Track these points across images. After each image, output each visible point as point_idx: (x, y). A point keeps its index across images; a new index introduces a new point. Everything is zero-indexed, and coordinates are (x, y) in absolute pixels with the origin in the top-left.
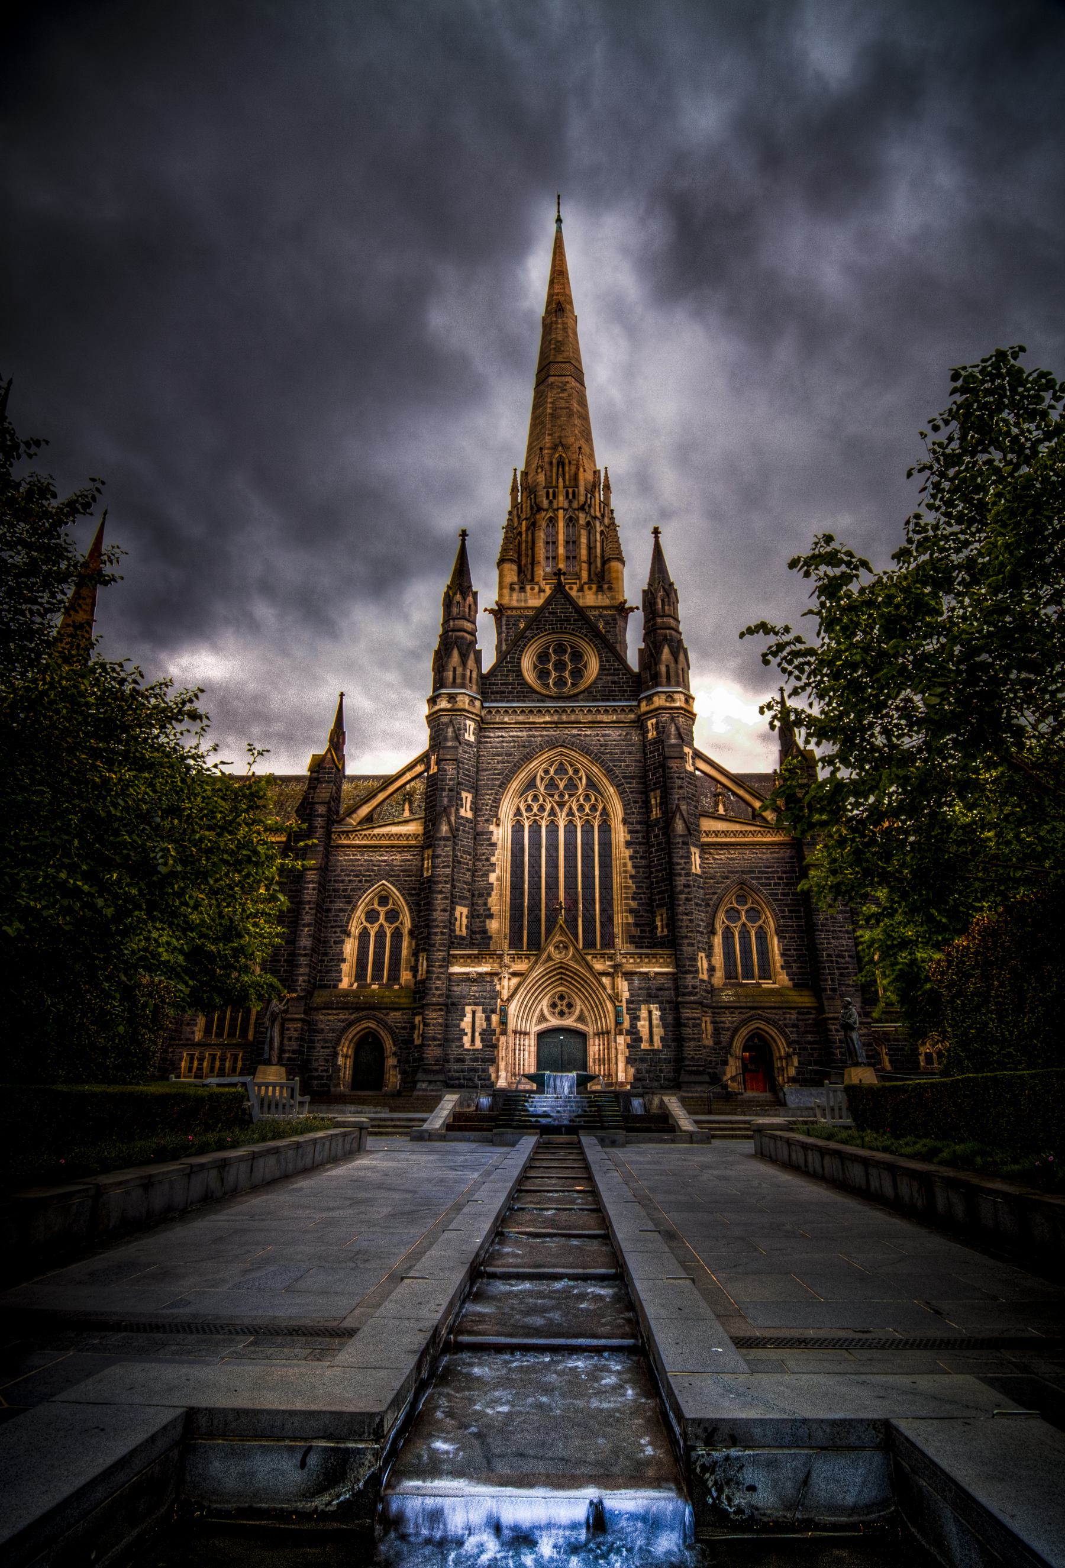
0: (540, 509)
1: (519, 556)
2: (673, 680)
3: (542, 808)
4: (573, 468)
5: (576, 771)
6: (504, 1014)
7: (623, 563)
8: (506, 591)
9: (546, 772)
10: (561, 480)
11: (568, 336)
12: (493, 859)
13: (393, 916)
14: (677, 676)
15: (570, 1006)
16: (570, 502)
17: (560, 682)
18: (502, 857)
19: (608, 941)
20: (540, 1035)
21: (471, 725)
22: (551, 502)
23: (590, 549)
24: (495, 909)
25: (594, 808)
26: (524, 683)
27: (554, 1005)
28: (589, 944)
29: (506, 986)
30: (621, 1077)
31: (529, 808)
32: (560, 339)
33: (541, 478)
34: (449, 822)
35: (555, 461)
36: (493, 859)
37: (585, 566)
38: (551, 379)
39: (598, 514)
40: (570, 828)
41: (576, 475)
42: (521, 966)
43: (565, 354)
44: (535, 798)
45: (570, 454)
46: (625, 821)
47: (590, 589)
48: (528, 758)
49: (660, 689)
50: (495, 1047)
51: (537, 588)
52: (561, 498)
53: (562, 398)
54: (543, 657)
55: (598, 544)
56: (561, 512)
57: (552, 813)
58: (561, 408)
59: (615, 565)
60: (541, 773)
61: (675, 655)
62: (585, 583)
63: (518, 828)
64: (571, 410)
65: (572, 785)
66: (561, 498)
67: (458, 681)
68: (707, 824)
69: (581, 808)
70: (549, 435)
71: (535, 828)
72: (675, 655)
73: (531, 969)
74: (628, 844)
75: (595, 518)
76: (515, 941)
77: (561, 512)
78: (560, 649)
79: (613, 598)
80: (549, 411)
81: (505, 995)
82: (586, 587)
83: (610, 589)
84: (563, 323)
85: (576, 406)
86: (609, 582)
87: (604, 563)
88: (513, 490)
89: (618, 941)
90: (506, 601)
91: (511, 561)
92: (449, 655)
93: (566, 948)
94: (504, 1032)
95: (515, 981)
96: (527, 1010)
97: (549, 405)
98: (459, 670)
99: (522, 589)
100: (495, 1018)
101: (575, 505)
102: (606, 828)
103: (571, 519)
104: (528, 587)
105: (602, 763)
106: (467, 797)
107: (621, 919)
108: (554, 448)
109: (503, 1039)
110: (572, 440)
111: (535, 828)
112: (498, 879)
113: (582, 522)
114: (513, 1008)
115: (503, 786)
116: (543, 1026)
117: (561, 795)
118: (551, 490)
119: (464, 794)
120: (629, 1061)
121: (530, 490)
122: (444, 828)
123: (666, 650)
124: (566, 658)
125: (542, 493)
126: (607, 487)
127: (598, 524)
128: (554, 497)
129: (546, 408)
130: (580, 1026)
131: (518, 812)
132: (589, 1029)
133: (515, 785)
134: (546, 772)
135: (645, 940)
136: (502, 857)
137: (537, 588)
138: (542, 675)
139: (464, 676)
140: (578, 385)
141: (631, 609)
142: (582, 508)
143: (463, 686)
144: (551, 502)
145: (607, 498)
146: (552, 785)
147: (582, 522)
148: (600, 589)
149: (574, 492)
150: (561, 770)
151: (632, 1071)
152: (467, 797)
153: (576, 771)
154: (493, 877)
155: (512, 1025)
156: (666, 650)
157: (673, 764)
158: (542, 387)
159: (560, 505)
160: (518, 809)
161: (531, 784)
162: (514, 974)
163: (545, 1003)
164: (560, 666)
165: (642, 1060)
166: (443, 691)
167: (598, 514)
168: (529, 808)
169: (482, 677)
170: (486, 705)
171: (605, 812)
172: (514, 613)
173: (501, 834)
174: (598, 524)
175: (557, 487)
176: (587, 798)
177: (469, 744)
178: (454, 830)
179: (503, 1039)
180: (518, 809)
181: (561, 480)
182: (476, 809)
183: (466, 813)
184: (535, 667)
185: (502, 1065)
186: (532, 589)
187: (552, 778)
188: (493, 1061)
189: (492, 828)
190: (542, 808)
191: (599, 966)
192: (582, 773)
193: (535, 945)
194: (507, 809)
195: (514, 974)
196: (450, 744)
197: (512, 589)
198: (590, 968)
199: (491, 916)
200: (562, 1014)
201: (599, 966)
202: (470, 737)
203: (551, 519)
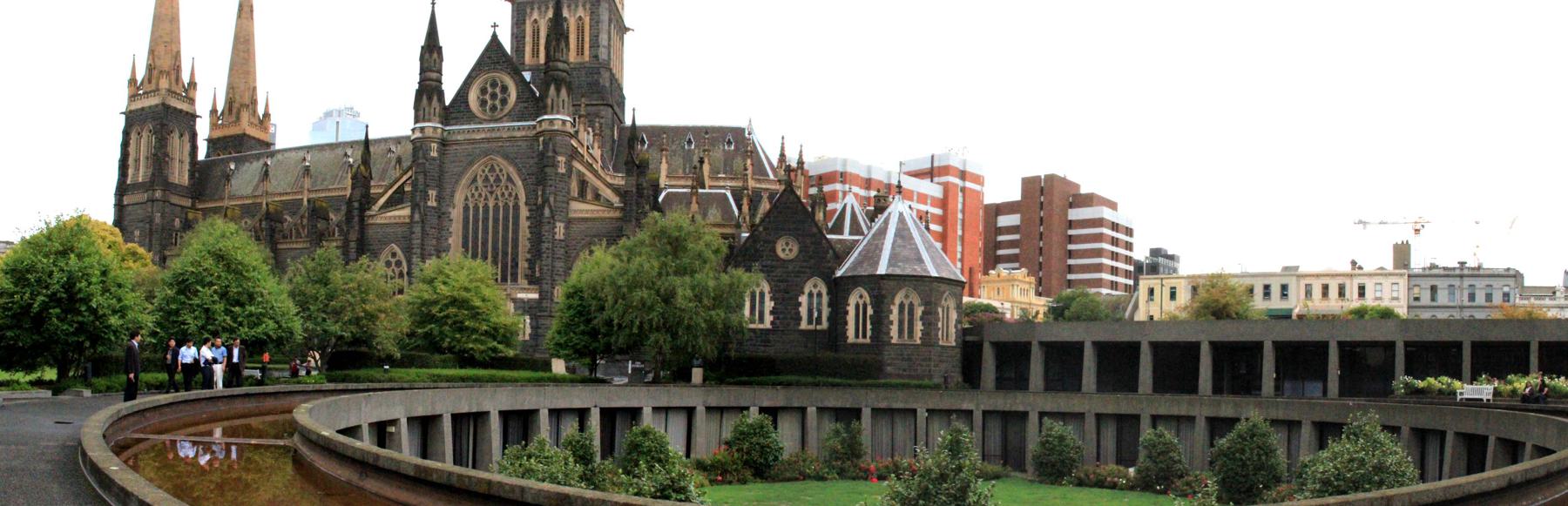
13: (399, 264)
17: (494, 108)
19: (515, 280)
21: (434, 146)
26: (469, 111)
48: (471, 164)
63: (466, 208)
65: (498, 180)
68: (575, 205)
71: (476, 208)
78: (494, 85)
102: (516, 207)
105: (516, 165)
106: (432, 193)
107: (523, 265)
111: (476, 208)
115: (457, 182)
124: (498, 90)
133: (464, 181)
135: (533, 280)
138: (483, 103)
146: (486, 179)
150: (492, 169)
152: (432, 193)
154: (450, 241)
157: (548, 170)
161: (474, 180)
164: (494, 96)
169: (445, 108)
171: (516, 197)
173: (456, 213)
177: (434, 159)
183: (432, 203)
194: (459, 198)
202: (434, 154)
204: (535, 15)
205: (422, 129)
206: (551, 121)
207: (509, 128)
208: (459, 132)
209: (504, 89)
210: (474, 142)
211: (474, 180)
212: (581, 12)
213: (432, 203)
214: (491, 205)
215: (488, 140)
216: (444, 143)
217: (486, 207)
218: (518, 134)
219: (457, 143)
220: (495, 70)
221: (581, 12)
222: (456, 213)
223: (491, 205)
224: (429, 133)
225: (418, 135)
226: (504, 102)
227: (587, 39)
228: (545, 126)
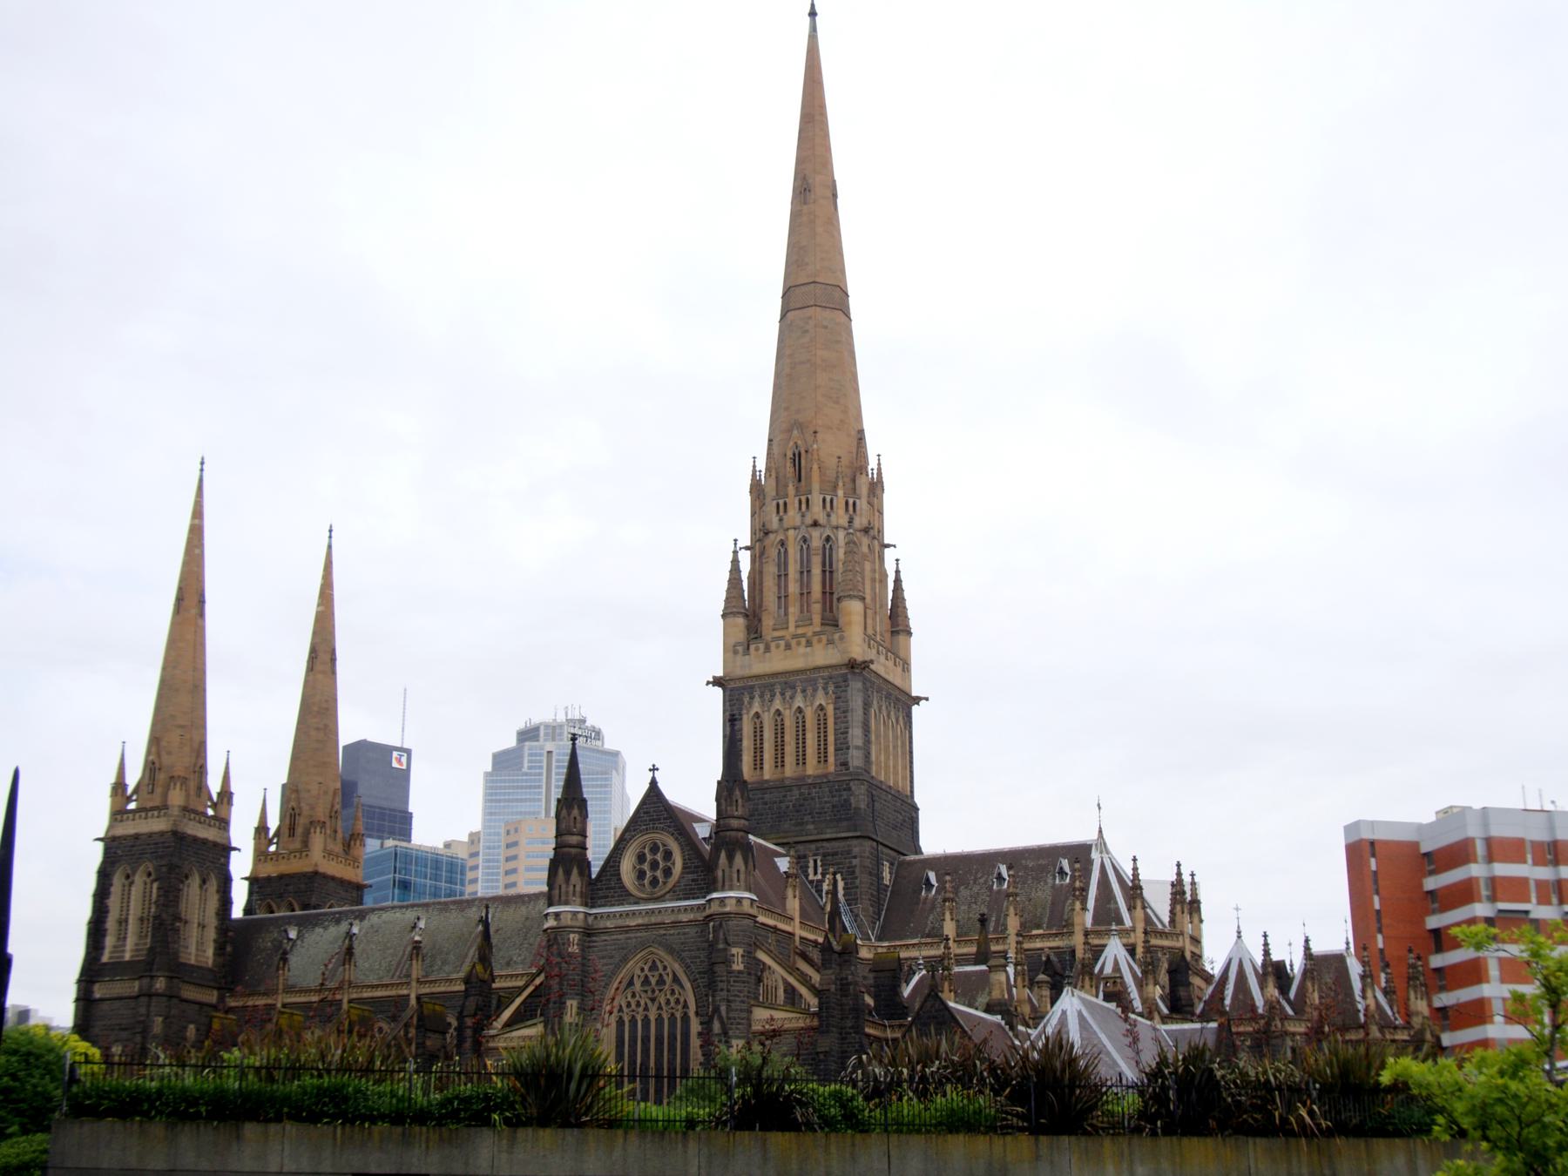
3: (638, 1005)
5: (665, 968)
22: (781, 520)
25: (677, 1001)
31: (629, 1005)
44: (634, 995)
46: (697, 1014)
47: (820, 641)
48: (625, 960)
49: (715, 895)
57: (646, 1009)
60: (638, 972)
63: (620, 1022)
65: (661, 981)
71: (633, 1021)
77: (791, 533)
78: (654, 849)
101: (809, 521)
104: (752, 647)
105: (682, 961)
111: (633, 1021)
124: (659, 857)
138: (641, 875)
143: (567, 903)
146: (646, 981)
150: (653, 967)
153: (665, 968)
157: (718, 968)
159: (791, 524)
164: (654, 865)
168: (629, 1005)
171: (686, 1006)
176: (673, 992)
186: (757, 649)
190: (638, 1005)
202: (574, 949)
205: (557, 915)
206: (722, 900)
207: (673, 910)
208: (609, 915)
209: (668, 855)
210: (627, 930)
211: (631, 983)
212: (820, 699)
214: (652, 1018)
215: (646, 927)
216: (588, 933)
217: (646, 1020)
218: (684, 917)
219: (606, 931)
221: (820, 699)
223: (652, 1018)
224: (567, 920)
226: (668, 872)
227: (831, 738)
228: (715, 908)
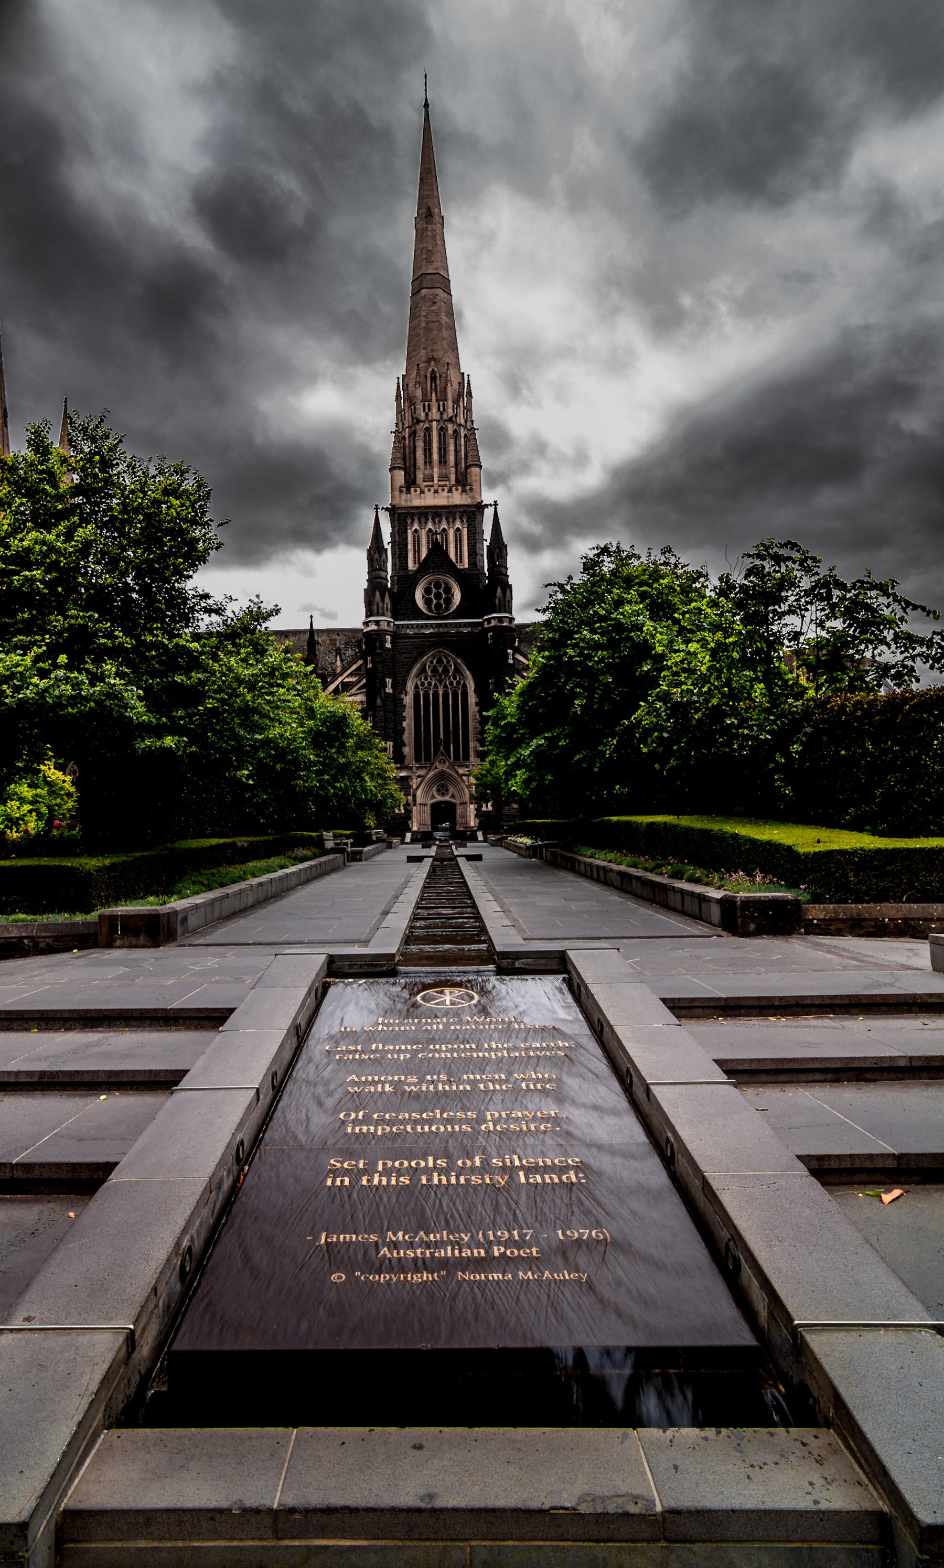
0: (419, 421)
1: (405, 464)
2: (503, 608)
3: (430, 684)
4: (443, 380)
5: (448, 662)
6: (414, 796)
7: (481, 467)
8: (397, 493)
9: (432, 662)
10: (434, 394)
11: (436, 245)
12: (404, 714)
14: (505, 606)
15: (447, 790)
16: (441, 414)
17: (438, 606)
18: (409, 713)
19: (466, 757)
20: (433, 805)
21: (388, 638)
22: (427, 415)
23: (457, 452)
24: (406, 741)
25: (458, 683)
27: (438, 791)
28: (457, 757)
29: (414, 783)
30: (472, 824)
31: (423, 684)
32: (430, 248)
33: (419, 393)
34: (381, 698)
35: (429, 375)
36: (404, 714)
37: (453, 470)
38: (424, 292)
39: (462, 422)
40: (446, 695)
41: (445, 388)
42: (422, 772)
43: (435, 265)
44: (426, 679)
45: (440, 367)
47: (457, 490)
48: (422, 655)
49: (495, 615)
50: (411, 811)
51: (418, 489)
52: (434, 410)
53: (433, 311)
54: (427, 591)
55: (463, 448)
56: (434, 423)
57: (436, 686)
58: (433, 322)
59: (474, 470)
60: (428, 663)
61: (504, 592)
62: (453, 485)
63: (417, 696)
64: (441, 324)
65: (446, 671)
66: (434, 410)
67: (380, 611)
69: (451, 683)
70: (424, 348)
71: (426, 695)
72: (504, 592)
73: (427, 774)
74: (477, 704)
75: (460, 425)
76: (418, 759)
77: (434, 423)
78: (438, 585)
79: (473, 498)
80: (423, 325)
81: (414, 787)
82: (454, 488)
83: (471, 489)
84: (433, 230)
85: (444, 319)
86: (471, 485)
87: (467, 468)
88: (397, 399)
89: (472, 759)
90: (396, 502)
91: (400, 468)
92: (374, 595)
93: (444, 762)
94: (415, 805)
95: (419, 779)
96: (426, 792)
97: (423, 319)
98: (380, 605)
99: (408, 491)
100: (410, 798)
101: (445, 417)
103: (442, 428)
104: (412, 490)
105: (463, 659)
106: (389, 681)
108: (429, 360)
109: (414, 808)
110: (441, 353)
111: (426, 695)
112: (408, 725)
113: (450, 431)
114: (419, 793)
115: (408, 672)
116: (434, 800)
117: (440, 676)
118: (426, 404)
119: (387, 680)
120: (476, 816)
121: (410, 400)
122: (379, 701)
123: (499, 590)
125: (420, 407)
126: (470, 394)
127: (462, 429)
128: (429, 410)
129: (420, 321)
130: (452, 800)
131: (416, 687)
132: (457, 801)
133: (415, 671)
134: (432, 662)
136: (409, 713)
137: (418, 489)
138: (428, 602)
139: (383, 609)
140: (446, 295)
141: (486, 506)
142: (450, 420)
143: (383, 615)
144: (427, 415)
145: (470, 402)
146: (434, 670)
147: (450, 431)
148: (464, 491)
149: (444, 405)
150: (440, 661)
151: (478, 821)
152: (389, 681)
154: (404, 724)
155: (419, 800)
156: (499, 590)
158: (417, 298)
159: (434, 417)
160: (417, 684)
161: (423, 670)
162: (419, 776)
163: (435, 789)
164: (438, 596)
165: (482, 816)
166: (372, 619)
167: (462, 422)
168: (423, 684)
170: (396, 623)
171: (465, 686)
172: (403, 511)
173: (408, 700)
174: (462, 429)
175: (431, 401)
178: (383, 701)
179: (414, 808)
180: (417, 684)
181: (434, 394)
182: (393, 686)
183: (389, 690)
184: (423, 597)
185: (415, 820)
187: (435, 666)
188: (410, 818)
189: (403, 696)
190: (430, 684)
191: (461, 771)
192: (452, 662)
193: (428, 759)
194: (410, 686)
195: (419, 776)
196: (378, 651)
197: (401, 492)
198: (457, 772)
199: (405, 745)
200: (443, 795)
201: (461, 771)
202: (388, 645)
203: (427, 429)
204: (416, 526)
206: (500, 619)
208: (408, 626)
209: (448, 590)
212: (458, 525)
213: (389, 690)
216: (396, 636)
219: (406, 636)
220: (440, 573)
221: (458, 525)
222: (408, 700)
224: (384, 626)
225: (373, 627)
228: (493, 623)
